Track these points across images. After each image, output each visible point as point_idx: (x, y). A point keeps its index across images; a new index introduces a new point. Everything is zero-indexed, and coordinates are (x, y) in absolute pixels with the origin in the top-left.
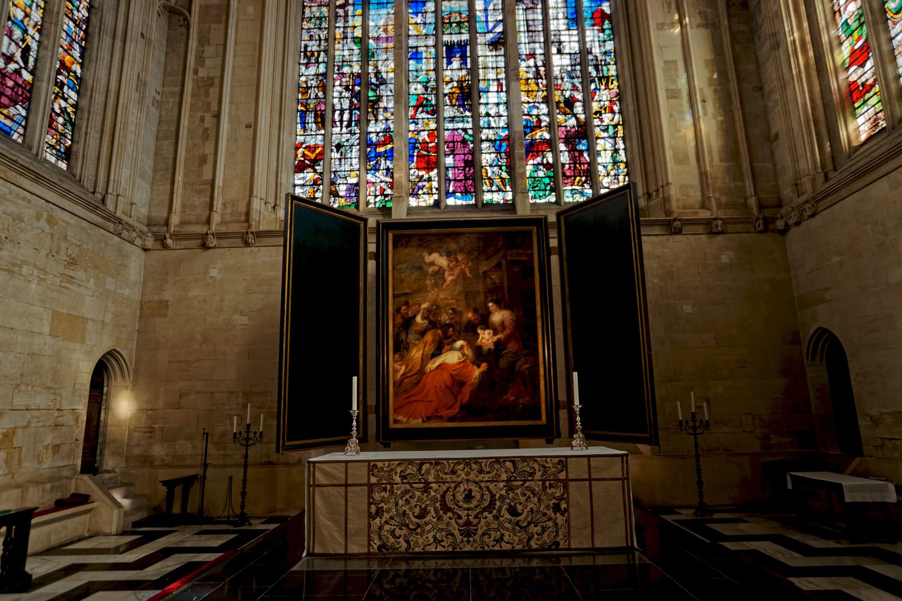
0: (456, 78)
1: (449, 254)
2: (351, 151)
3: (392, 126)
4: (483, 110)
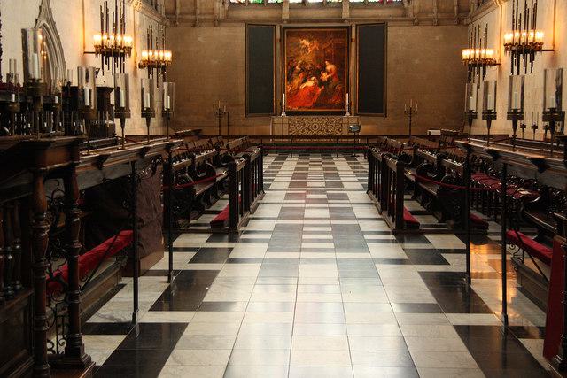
1: (310, 40)
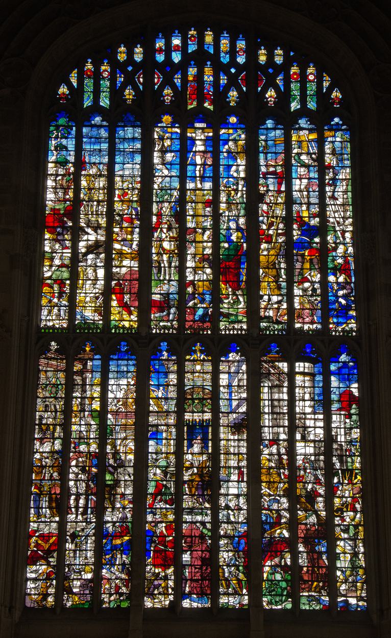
0: (196, 464)
2: (87, 543)
3: (129, 515)
4: (222, 502)
